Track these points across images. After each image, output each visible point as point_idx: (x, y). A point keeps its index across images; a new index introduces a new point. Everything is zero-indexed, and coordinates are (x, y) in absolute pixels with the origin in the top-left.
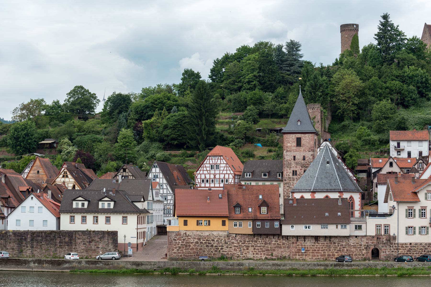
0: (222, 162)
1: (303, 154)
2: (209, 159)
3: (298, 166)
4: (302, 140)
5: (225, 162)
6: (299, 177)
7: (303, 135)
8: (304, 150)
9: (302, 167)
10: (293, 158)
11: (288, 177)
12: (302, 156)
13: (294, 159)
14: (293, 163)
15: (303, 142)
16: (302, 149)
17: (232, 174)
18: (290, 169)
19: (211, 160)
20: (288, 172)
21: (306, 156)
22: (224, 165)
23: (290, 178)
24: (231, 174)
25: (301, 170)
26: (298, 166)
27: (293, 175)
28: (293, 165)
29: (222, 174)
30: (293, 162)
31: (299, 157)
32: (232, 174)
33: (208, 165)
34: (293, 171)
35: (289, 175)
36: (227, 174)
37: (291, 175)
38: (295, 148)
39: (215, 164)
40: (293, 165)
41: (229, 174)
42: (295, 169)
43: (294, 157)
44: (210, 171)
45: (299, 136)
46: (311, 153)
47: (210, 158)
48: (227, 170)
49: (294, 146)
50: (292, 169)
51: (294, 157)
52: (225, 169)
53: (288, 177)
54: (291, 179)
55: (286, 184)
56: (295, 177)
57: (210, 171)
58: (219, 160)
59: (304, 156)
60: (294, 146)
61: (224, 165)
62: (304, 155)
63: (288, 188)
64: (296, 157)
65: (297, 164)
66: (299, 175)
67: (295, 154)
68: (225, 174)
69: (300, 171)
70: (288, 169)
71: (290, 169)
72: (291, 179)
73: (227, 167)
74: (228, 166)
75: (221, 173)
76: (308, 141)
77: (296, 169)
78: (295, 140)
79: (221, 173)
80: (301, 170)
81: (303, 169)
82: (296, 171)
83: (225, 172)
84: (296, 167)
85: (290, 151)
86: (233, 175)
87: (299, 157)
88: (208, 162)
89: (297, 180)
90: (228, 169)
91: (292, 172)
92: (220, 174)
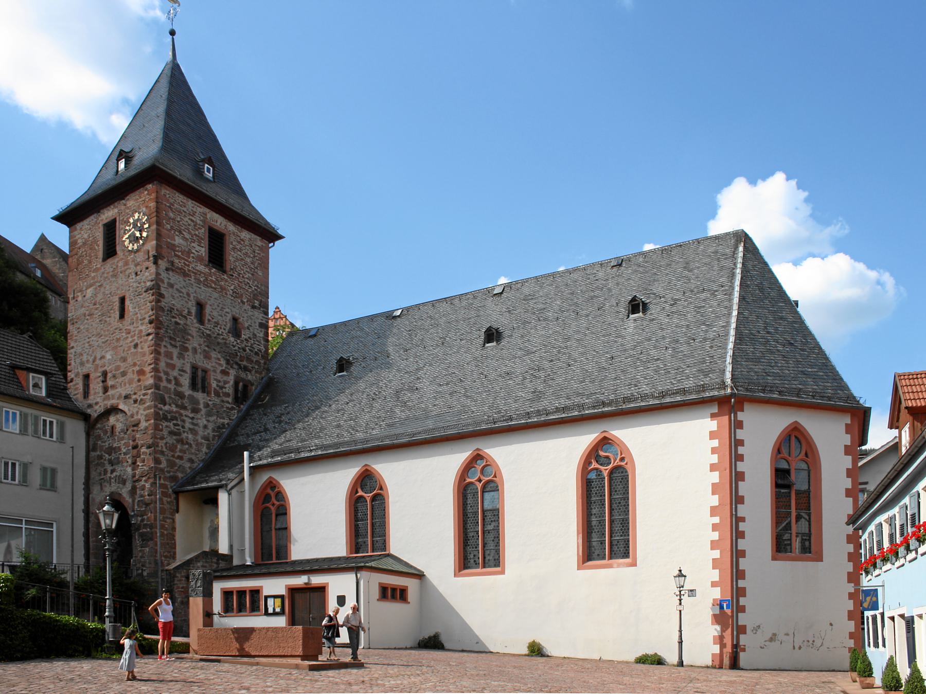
6: (217, 401)
11: (172, 386)
14: (193, 331)
15: (231, 257)
21: (244, 321)
25: (224, 372)
27: (194, 386)
37: (186, 381)
38: (201, 268)
40: (195, 342)
46: (258, 315)
49: (200, 259)
51: (200, 306)
55: (165, 418)
56: (200, 396)
59: (235, 320)
60: (200, 259)
63: (171, 440)
64: (208, 310)
65: (210, 340)
67: (204, 293)
69: (219, 376)
71: (181, 356)
81: (233, 372)
84: (207, 356)
91: (188, 368)
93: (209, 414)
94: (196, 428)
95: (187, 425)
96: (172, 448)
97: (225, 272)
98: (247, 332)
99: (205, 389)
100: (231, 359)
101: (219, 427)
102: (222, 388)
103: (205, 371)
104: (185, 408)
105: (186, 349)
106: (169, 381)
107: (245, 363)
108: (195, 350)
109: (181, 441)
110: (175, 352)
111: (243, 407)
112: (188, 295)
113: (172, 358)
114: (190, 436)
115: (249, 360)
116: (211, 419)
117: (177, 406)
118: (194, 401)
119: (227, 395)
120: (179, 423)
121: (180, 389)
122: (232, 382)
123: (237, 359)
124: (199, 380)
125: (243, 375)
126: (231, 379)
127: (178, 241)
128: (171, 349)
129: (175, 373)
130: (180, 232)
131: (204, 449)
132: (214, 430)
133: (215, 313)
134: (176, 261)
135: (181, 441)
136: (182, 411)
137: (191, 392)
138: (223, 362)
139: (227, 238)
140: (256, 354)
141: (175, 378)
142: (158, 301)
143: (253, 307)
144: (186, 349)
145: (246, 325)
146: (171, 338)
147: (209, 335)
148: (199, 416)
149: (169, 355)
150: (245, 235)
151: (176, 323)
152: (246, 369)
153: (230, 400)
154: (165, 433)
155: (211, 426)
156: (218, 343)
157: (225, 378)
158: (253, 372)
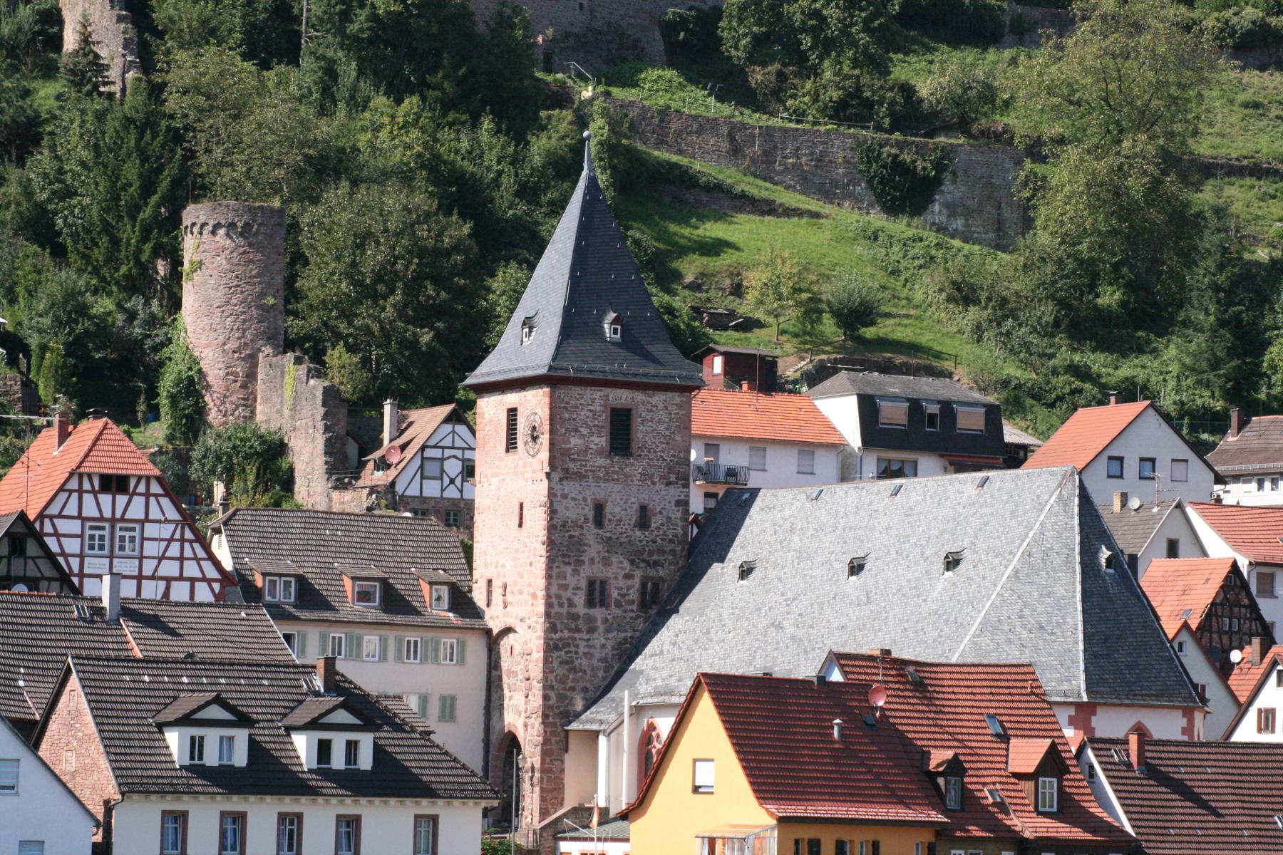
0: (155, 513)
1: (637, 495)
2: (81, 491)
3: (614, 559)
4: (636, 421)
5: (173, 514)
6: (618, 612)
7: (640, 396)
8: (646, 477)
9: (632, 562)
10: (591, 515)
12: (636, 507)
13: (599, 520)
14: (590, 539)
15: (641, 432)
16: (636, 468)
17: (209, 581)
18: (576, 572)
19: (88, 498)
20: (565, 587)
21: (656, 505)
22: (167, 531)
23: (575, 617)
24: (204, 579)
25: (628, 576)
26: (614, 559)
27: (590, 603)
28: (594, 550)
29: (152, 577)
30: (590, 532)
31: (621, 507)
32: (209, 581)
33: (75, 527)
34: (591, 583)
35: (571, 603)
36: (181, 578)
37: (580, 599)
38: (601, 462)
39: (113, 521)
40: (594, 550)
41: (193, 581)
42: (598, 571)
43: (599, 508)
44: (82, 557)
45: (622, 397)
46: (675, 492)
47: (87, 486)
48: (181, 559)
49: (599, 453)
50: (586, 571)
51: (599, 508)
52: (174, 550)
53: (564, 610)
54: (581, 623)
55: (556, 648)
56: (598, 613)
57: (82, 557)
58: (138, 502)
59: (643, 509)
60: (599, 453)
61: (167, 531)
62: (644, 497)
63: (561, 671)
64: (608, 510)
65: (610, 545)
66: (618, 604)
68: (169, 580)
69: (621, 582)
70: (569, 570)
71: (576, 572)
72: (581, 623)
73: (182, 540)
74: (189, 535)
75: (147, 571)
76: (662, 428)
77: (607, 573)
78: (604, 419)
79: (147, 571)
80: (628, 576)
81: (638, 574)
82: (603, 583)
83: (169, 568)
84: (606, 562)
85: (580, 476)
86: (217, 586)
87: (621, 507)
88: (72, 509)
89: (608, 630)
90: (188, 553)
91: (583, 584)
92: (140, 578)
93: (608, 630)
94: (592, 650)
95: (582, 650)
96: (562, 681)
97: (631, 455)
98: (659, 517)
99: (604, 603)
100: (637, 557)
101: (620, 644)
102: (623, 596)
103: (603, 583)
104: (579, 630)
105: (582, 562)
106: (561, 605)
107: (655, 557)
108: (592, 560)
109: (574, 670)
110: (569, 570)
111: (653, 612)
112: (585, 500)
113: (565, 578)
114: (585, 662)
115: (661, 551)
116: (610, 636)
117: (570, 630)
118: (590, 619)
119: (632, 602)
120: (572, 649)
121: (573, 610)
122: (637, 586)
123: (645, 556)
124: (597, 593)
125: (652, 573)
126: (636, 582)
127: (575, 441)
128: (564, 568)
129: (569, 594)
130: (577, 431)
131: (601, 674)
132: (613, 648)
133: (617, 509)
134: (571, 465)
135: (574, 670)
136: (576, 635)
137: (586, 611)
138: (626, 565)
139: (634, 412)
140: (671, 541)
141: (569, 600)
142: (551, 519)
143: (669, 484)
144: (582, 562)
145: (658, 509)
146: (564, 556)
147: (610, 538)
148: (596, 635)
149: (562, 576)
150: (659, 398)
151: (571, 537)
152: (657, 564)
153: (634, 607)
154: (555, 664)
155: (610, 644)
156: (621, 544)
157: (629, 582)
158: (666, 565)
